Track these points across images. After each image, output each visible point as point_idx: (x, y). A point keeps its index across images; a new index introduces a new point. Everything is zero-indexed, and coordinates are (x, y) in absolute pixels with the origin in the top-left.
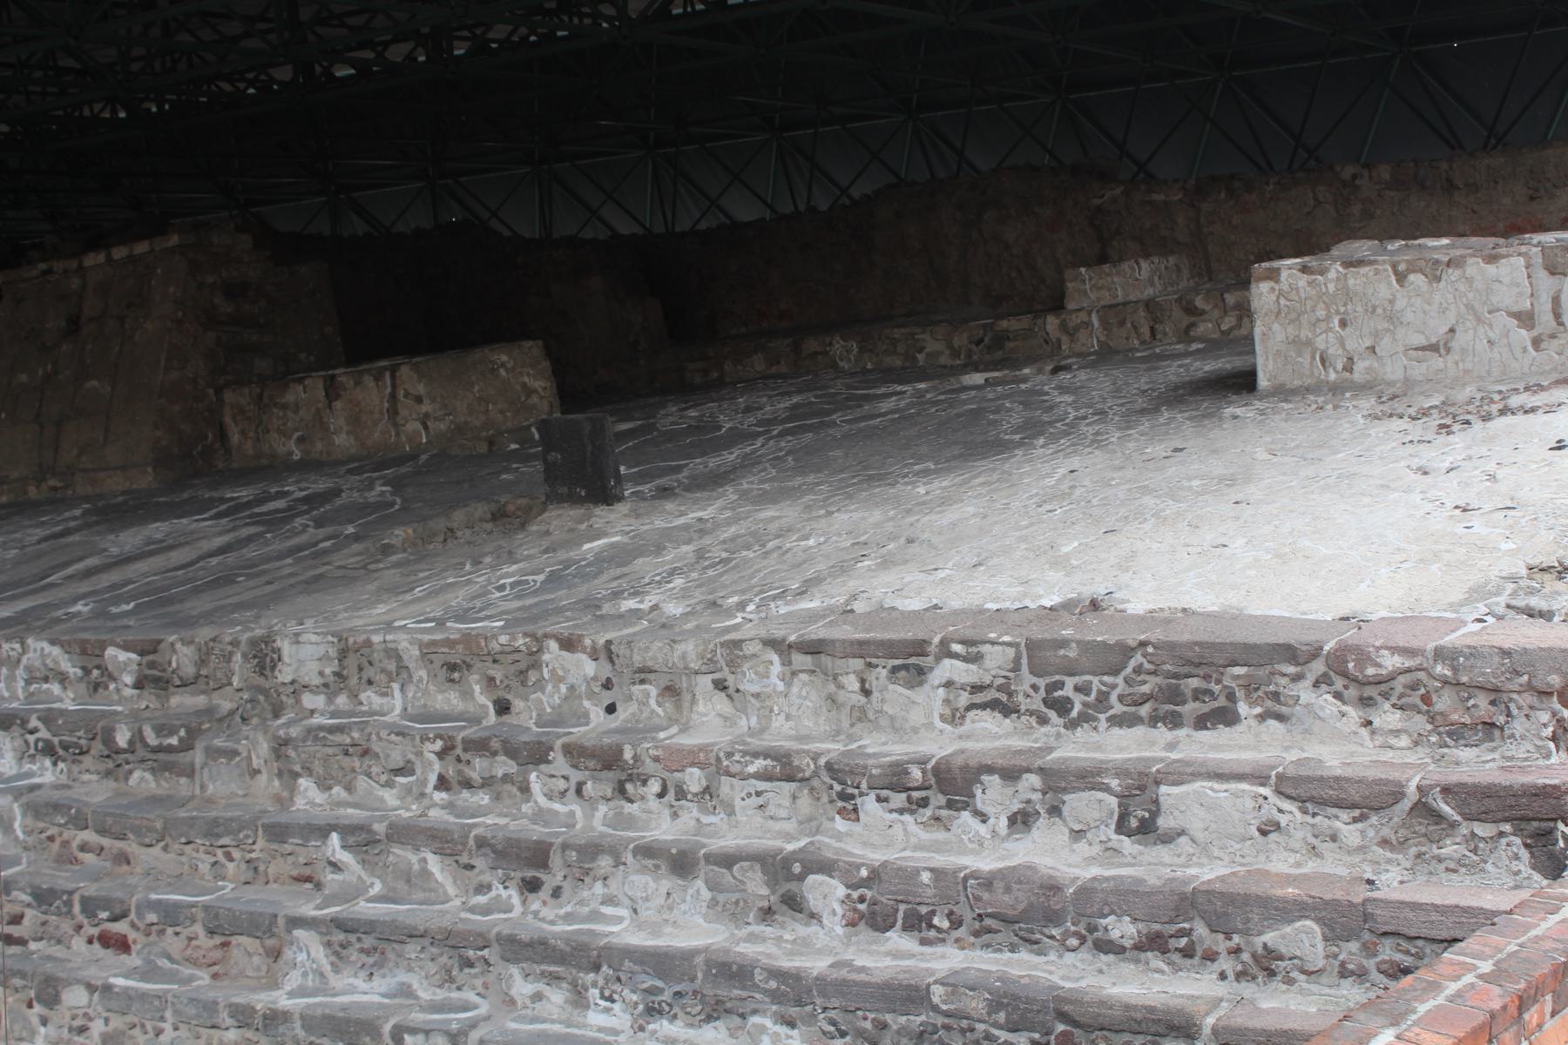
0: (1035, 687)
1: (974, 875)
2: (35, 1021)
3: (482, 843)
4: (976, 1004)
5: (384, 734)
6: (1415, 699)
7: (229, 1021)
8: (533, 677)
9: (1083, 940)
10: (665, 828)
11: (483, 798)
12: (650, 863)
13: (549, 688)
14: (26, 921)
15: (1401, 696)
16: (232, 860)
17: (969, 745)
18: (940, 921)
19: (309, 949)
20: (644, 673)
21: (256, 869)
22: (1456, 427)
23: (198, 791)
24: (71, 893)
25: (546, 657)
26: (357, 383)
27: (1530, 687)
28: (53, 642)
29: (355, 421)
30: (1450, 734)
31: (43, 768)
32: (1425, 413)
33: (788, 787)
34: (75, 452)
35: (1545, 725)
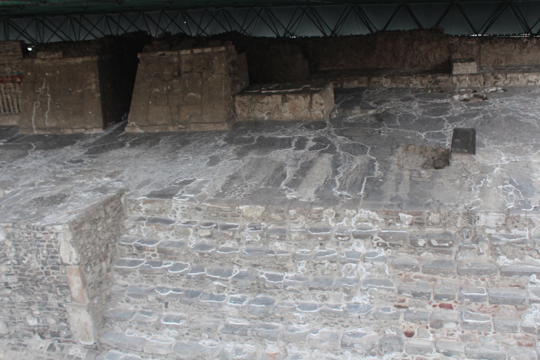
2: (429, 332)
16: (483, 280)
21: (494, 283)
24: (430, 294)
26: (296, 98)
28: (372, 211)
29: (293, 110)
34: (188, 117)
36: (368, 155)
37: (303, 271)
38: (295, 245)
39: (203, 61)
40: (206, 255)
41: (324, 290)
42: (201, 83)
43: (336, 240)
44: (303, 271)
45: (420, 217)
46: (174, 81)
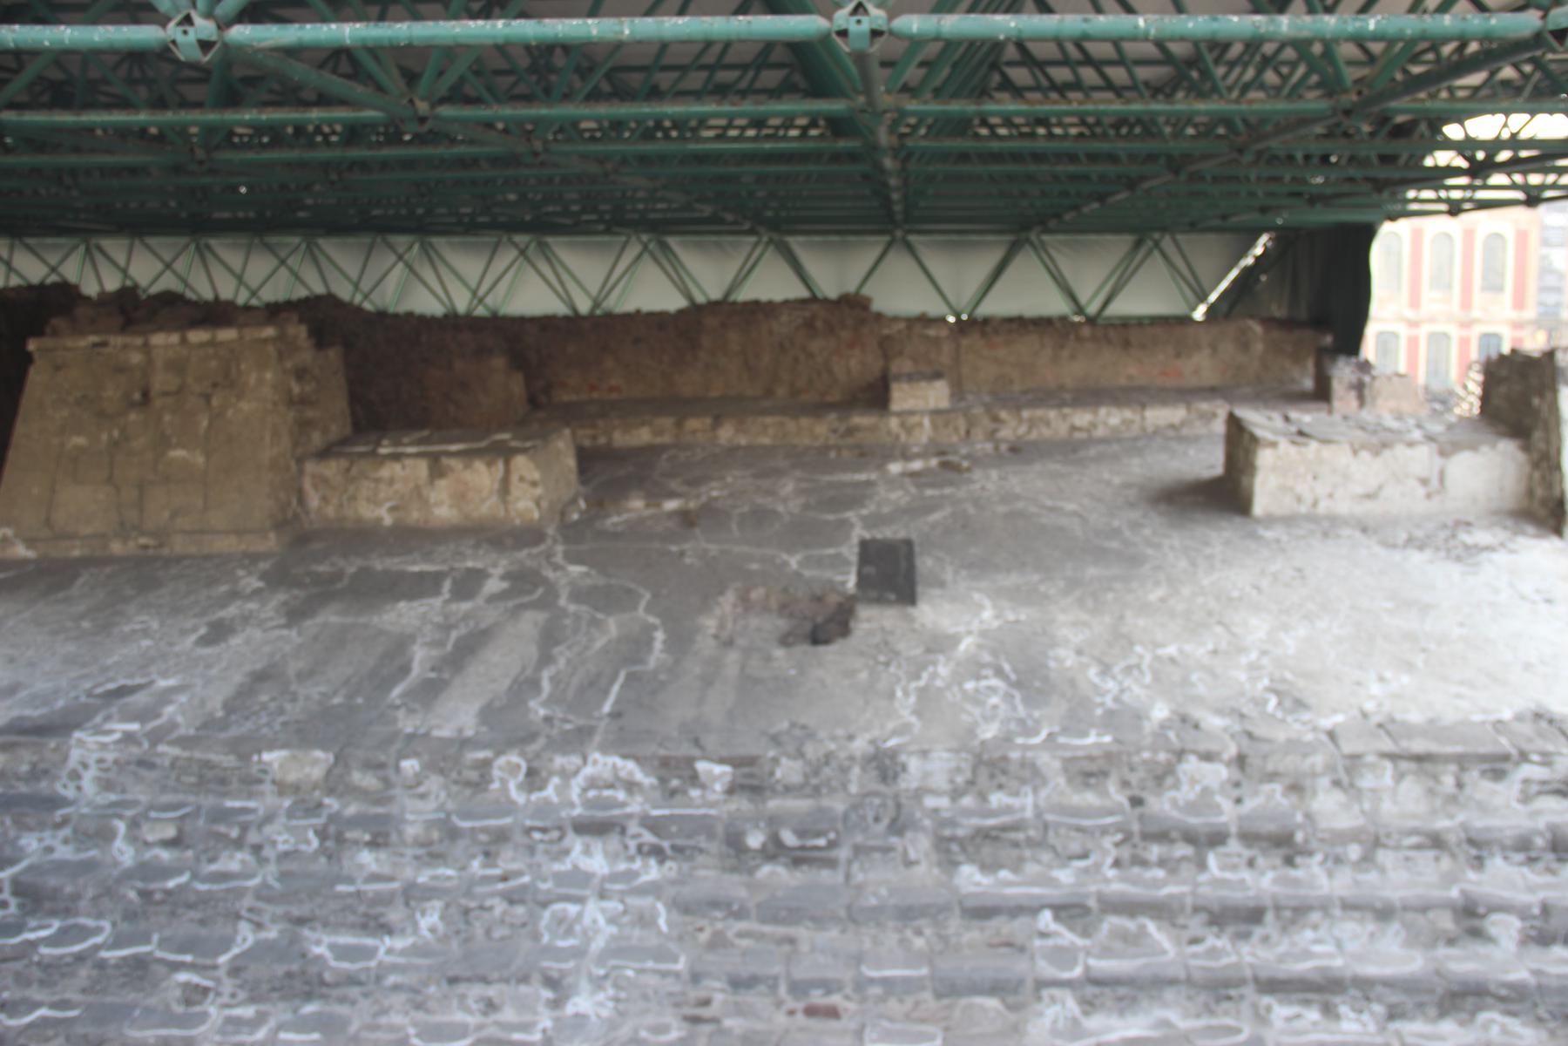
12: (1357, 915)
16: (919, 933)
20: (1272, 776)
24: (776, 978)
26: (467, 466)
28: (625, 757)
29: (460, 497)
31: (646, 867)
33: (1431, 854)
34: (166, 514)
36: (641, 611)
37: (433, 930)
38: (417, 858)
39: (214, 364)
40: (158, 896)
42: (205, 423)
43: (525, 840)
44: (433, 930)
45: (755, 770)
46: (133, 416)
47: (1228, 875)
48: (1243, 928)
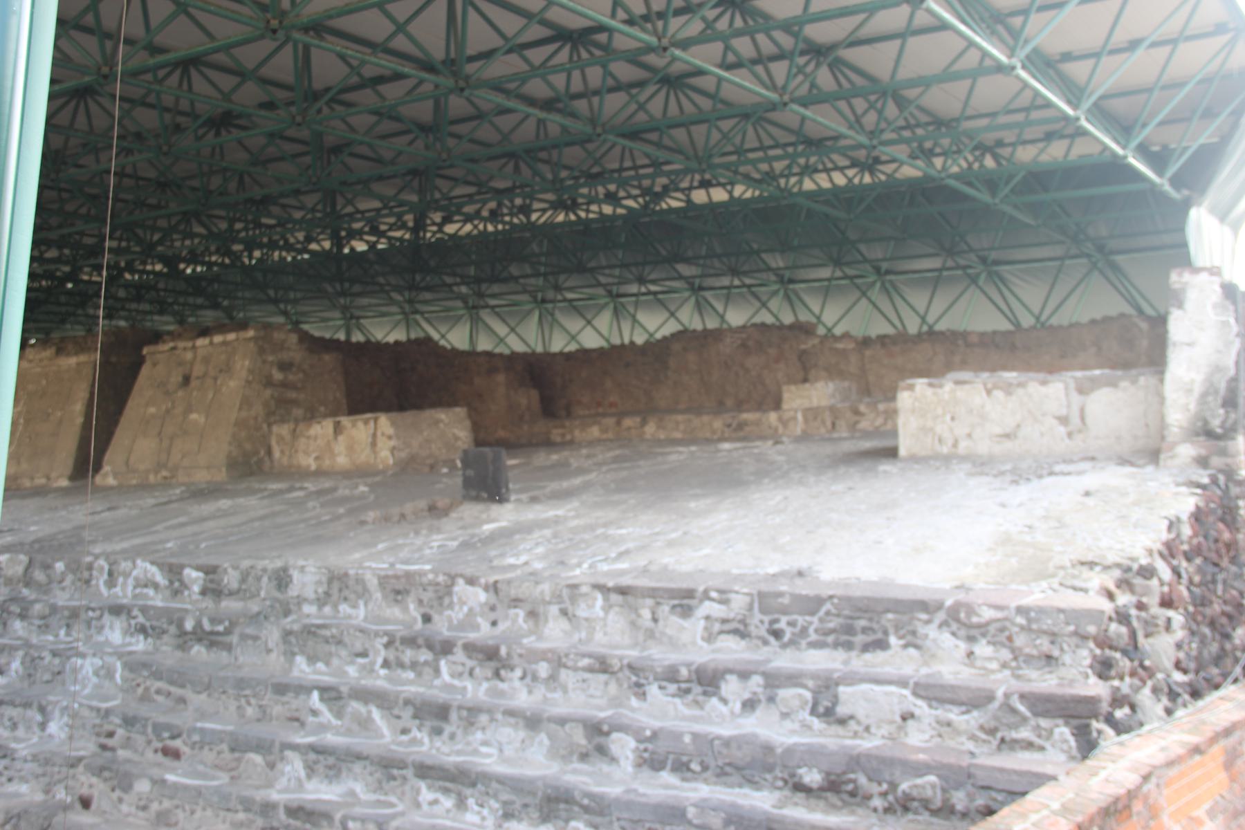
0: (762, 622)
1: (718, 737)
3: (407, 702)
4: (716, 821)
5: (352, 631)
6: (1002, 638)
7: (240, 807)
8: (446, 601)
9: (786, 782)
10: (523, 697)
11: (411, 675)
12: (512, 720)
13: (457, 608)
14: (117, 737)
15: (994, 636)
16: (249, 703)
17: (720, 656)
18: (695, 766)
19: (294, 766)
20: (516, 602)
21: (264, 712)
22: (1022, 482)
23: (233, 660)
24: (147, 720)
25: (456, 589)
27: (1076, 633)
28: (152, 563)
29: (350, 449)
30: (1025, 662)
31: (138, 641)
32: (1002, 473)
35: (1085, 658)
41: (15, 706)
44: (17, 672)
46: (180, 394)
47: (456, 682)
48: (436, 723)
